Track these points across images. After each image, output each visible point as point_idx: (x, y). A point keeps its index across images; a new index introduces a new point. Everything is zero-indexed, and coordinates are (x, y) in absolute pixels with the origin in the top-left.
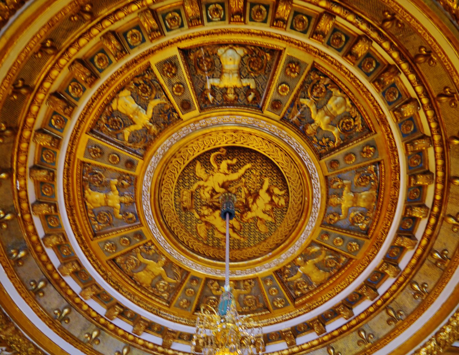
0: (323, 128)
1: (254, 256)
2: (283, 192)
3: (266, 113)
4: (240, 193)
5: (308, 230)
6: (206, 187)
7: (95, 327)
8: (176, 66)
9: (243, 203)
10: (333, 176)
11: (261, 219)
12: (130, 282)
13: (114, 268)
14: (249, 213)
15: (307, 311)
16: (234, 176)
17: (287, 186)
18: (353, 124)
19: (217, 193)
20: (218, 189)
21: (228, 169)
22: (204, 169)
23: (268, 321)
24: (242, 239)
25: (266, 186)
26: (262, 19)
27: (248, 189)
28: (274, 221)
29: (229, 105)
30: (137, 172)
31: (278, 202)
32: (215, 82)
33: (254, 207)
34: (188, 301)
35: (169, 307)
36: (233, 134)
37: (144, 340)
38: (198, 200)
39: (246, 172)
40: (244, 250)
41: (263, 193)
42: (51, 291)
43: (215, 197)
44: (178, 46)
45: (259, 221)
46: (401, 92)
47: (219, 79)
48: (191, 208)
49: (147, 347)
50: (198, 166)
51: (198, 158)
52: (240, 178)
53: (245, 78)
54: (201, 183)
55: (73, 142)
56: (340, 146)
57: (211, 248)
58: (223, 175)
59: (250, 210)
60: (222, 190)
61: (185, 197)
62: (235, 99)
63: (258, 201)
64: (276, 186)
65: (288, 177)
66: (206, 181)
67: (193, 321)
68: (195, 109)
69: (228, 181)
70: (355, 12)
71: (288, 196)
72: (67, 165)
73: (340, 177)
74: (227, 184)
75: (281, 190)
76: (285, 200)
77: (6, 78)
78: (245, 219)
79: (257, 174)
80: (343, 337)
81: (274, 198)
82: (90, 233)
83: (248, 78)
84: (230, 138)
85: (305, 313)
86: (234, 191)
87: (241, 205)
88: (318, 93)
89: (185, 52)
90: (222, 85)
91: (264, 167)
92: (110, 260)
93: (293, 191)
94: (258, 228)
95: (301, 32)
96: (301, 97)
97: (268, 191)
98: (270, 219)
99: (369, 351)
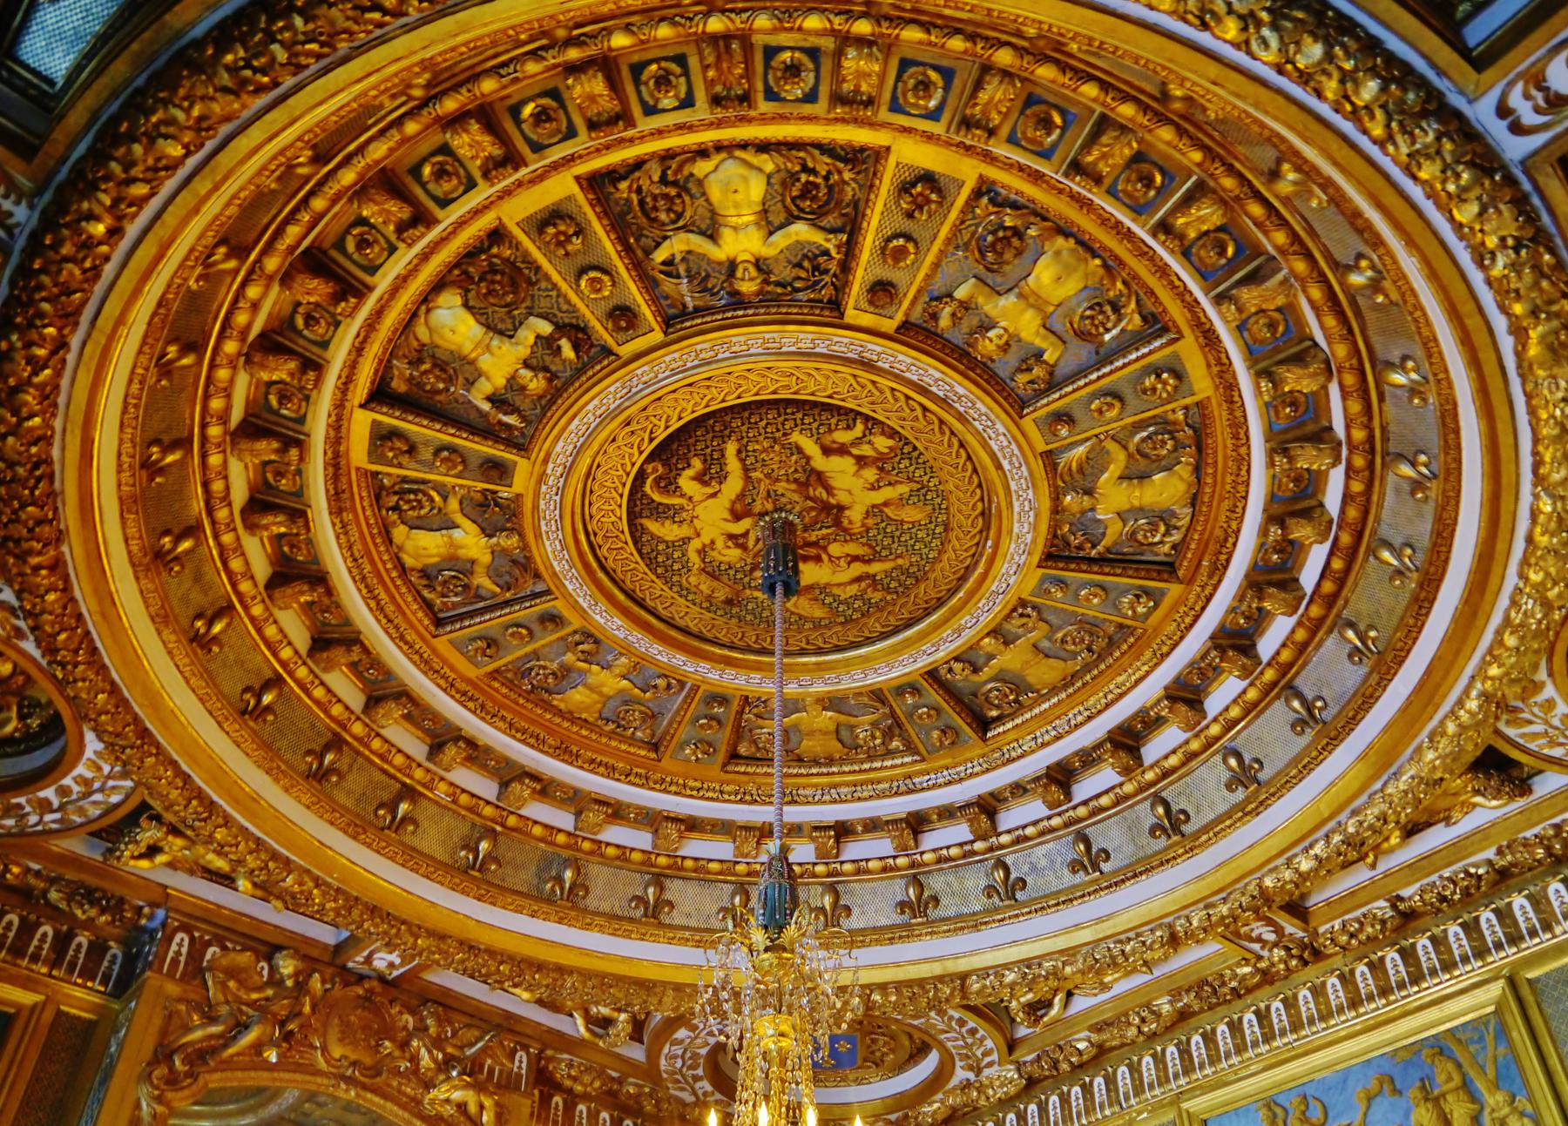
0: (768, 251)
1: (967, 568)
2: (859, 427)
3: (626, 350)
4: (784, 500)
5: (1002, 449)
6: (713, 542)
7: (820, 889)
8: (393, 434)
9: (812, 508)
10: (919, 308)
11: (886, 504)
12: (803, 771)
13: (750, 769)
14: (847, 513)
15: (1217, 577)
16: (733, 485)
17: (852, 410)
18: (819, 180)
19: (746, 534)
20: (738, 528)
21: (705, 484)
22: (668, 522)
23: (1154, 653)
24: (900, 561)
25: (811, 447)
26: (383, 249)
27: (788, 481)
28: (916, 486)
29: (552, 402)
30: (576, 622)
31: (875, 449)
32: (484, 387)
33: (842, 498)
34: (944, 732)
35: (923, 760)
36: (628, 429)
37: (934, 850)
38: (732, 572)
39: (742, 461)
40: (932, 576)
41: (819, 462)
42: (675, 889)
43: (751, 543)
44: (356, 402)
45: (886, 510)
46: (807, 45)
47: (483, 379)
48: (738, 593)
49: (949, 859)
50: (652, 526)
51: (632, 516)
52: (747, 478)
53: (516, 330)
54: (696, 544)
55: (431, 668)
56: (850, 249)
57: (865, 620)
58: (711, 501)
59: (841, 508)
60: (746, 524)
61: (703, 587)
62: (550, 381)
63: (833, 483)
64: (830, 431)
65: (830, 397)
66: (698, 535)
67: (997, 755)
68: (515, 463)
69: (733, 503)
70: (479, 69)
71: (876, 422)
72: (471, 705)
73: (936, 294)
74: (738, 507)
75: (849, 428)
76: (883, 433)
77: (219, 724)
78: (857, 528)
79: (766, 444)
80: (1356, 584)
81: (855, 451)
82: (643, 753)
83: (521, 323)
84: (635, 440)
85: (1216, 588)
86: (769, 506)
87: (813, 514)
88: (669, 210)
89: (380, 395)
90: (500, 382)
91: (763, 423)
92: (724, 765)
93: (878, 408)
94: (902, 522)
95: (465, 192)
96: (648, 252)
97: (827, 451)
98: (903, 489)
99: (1423, 595)
